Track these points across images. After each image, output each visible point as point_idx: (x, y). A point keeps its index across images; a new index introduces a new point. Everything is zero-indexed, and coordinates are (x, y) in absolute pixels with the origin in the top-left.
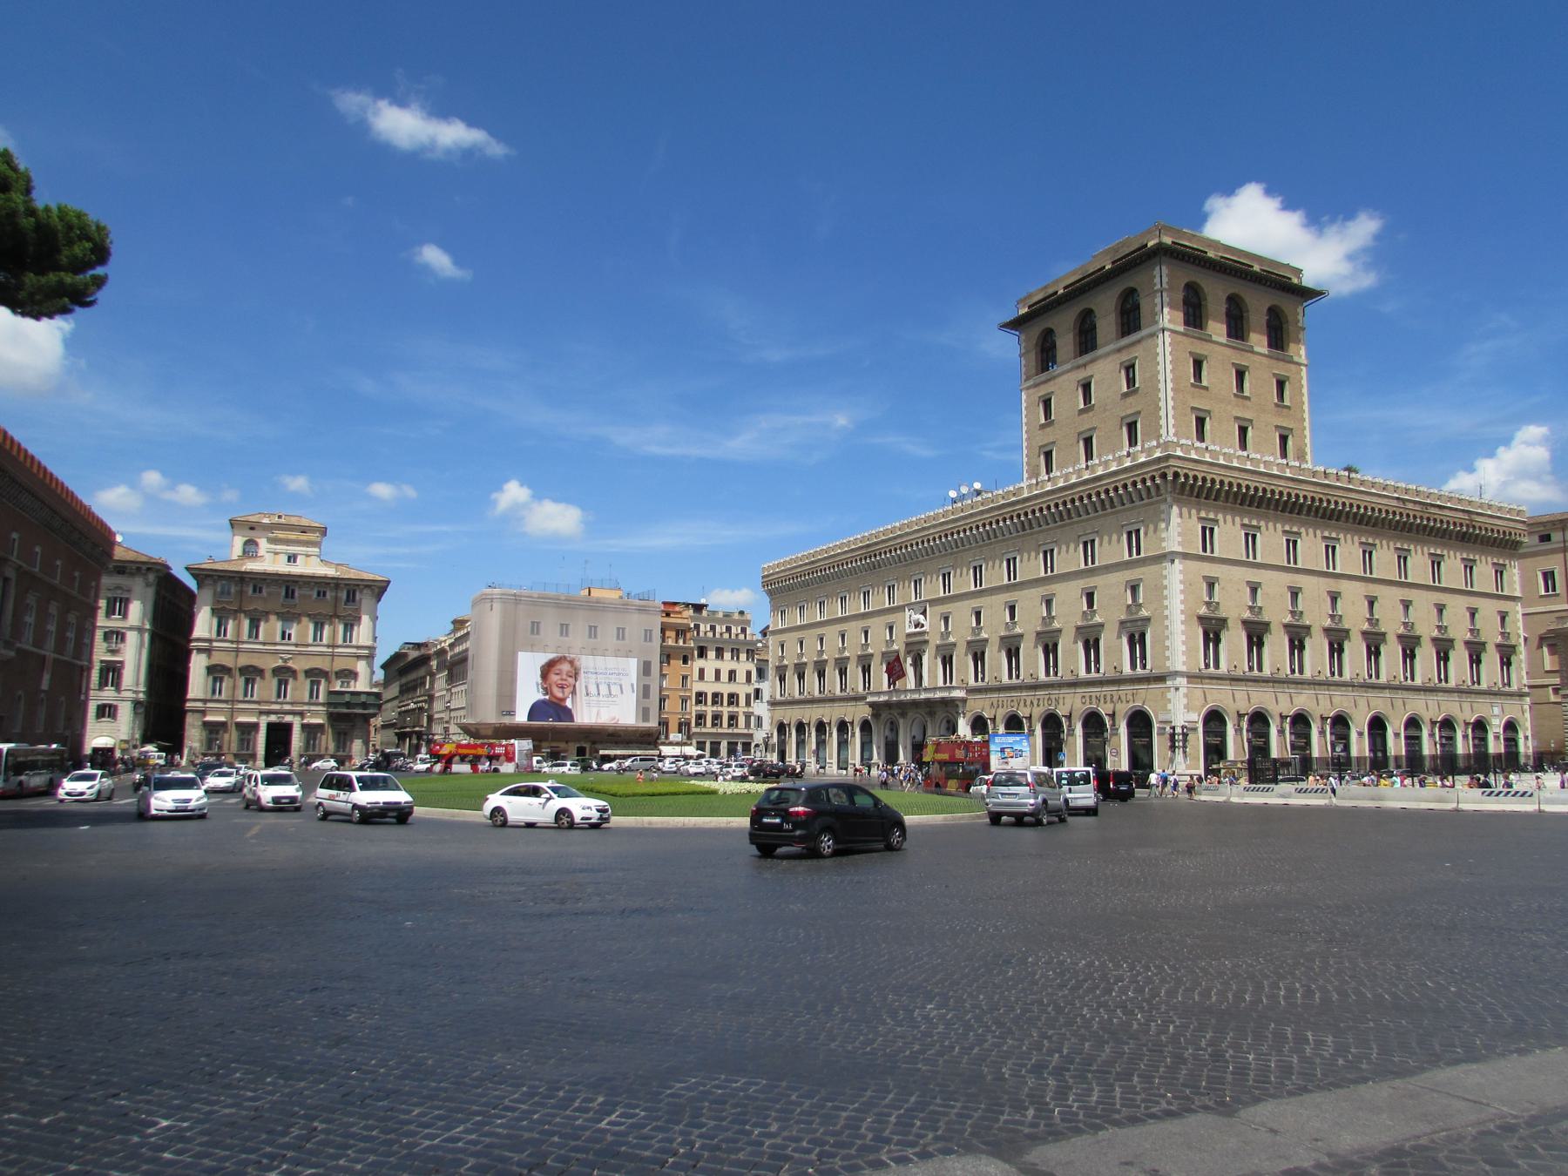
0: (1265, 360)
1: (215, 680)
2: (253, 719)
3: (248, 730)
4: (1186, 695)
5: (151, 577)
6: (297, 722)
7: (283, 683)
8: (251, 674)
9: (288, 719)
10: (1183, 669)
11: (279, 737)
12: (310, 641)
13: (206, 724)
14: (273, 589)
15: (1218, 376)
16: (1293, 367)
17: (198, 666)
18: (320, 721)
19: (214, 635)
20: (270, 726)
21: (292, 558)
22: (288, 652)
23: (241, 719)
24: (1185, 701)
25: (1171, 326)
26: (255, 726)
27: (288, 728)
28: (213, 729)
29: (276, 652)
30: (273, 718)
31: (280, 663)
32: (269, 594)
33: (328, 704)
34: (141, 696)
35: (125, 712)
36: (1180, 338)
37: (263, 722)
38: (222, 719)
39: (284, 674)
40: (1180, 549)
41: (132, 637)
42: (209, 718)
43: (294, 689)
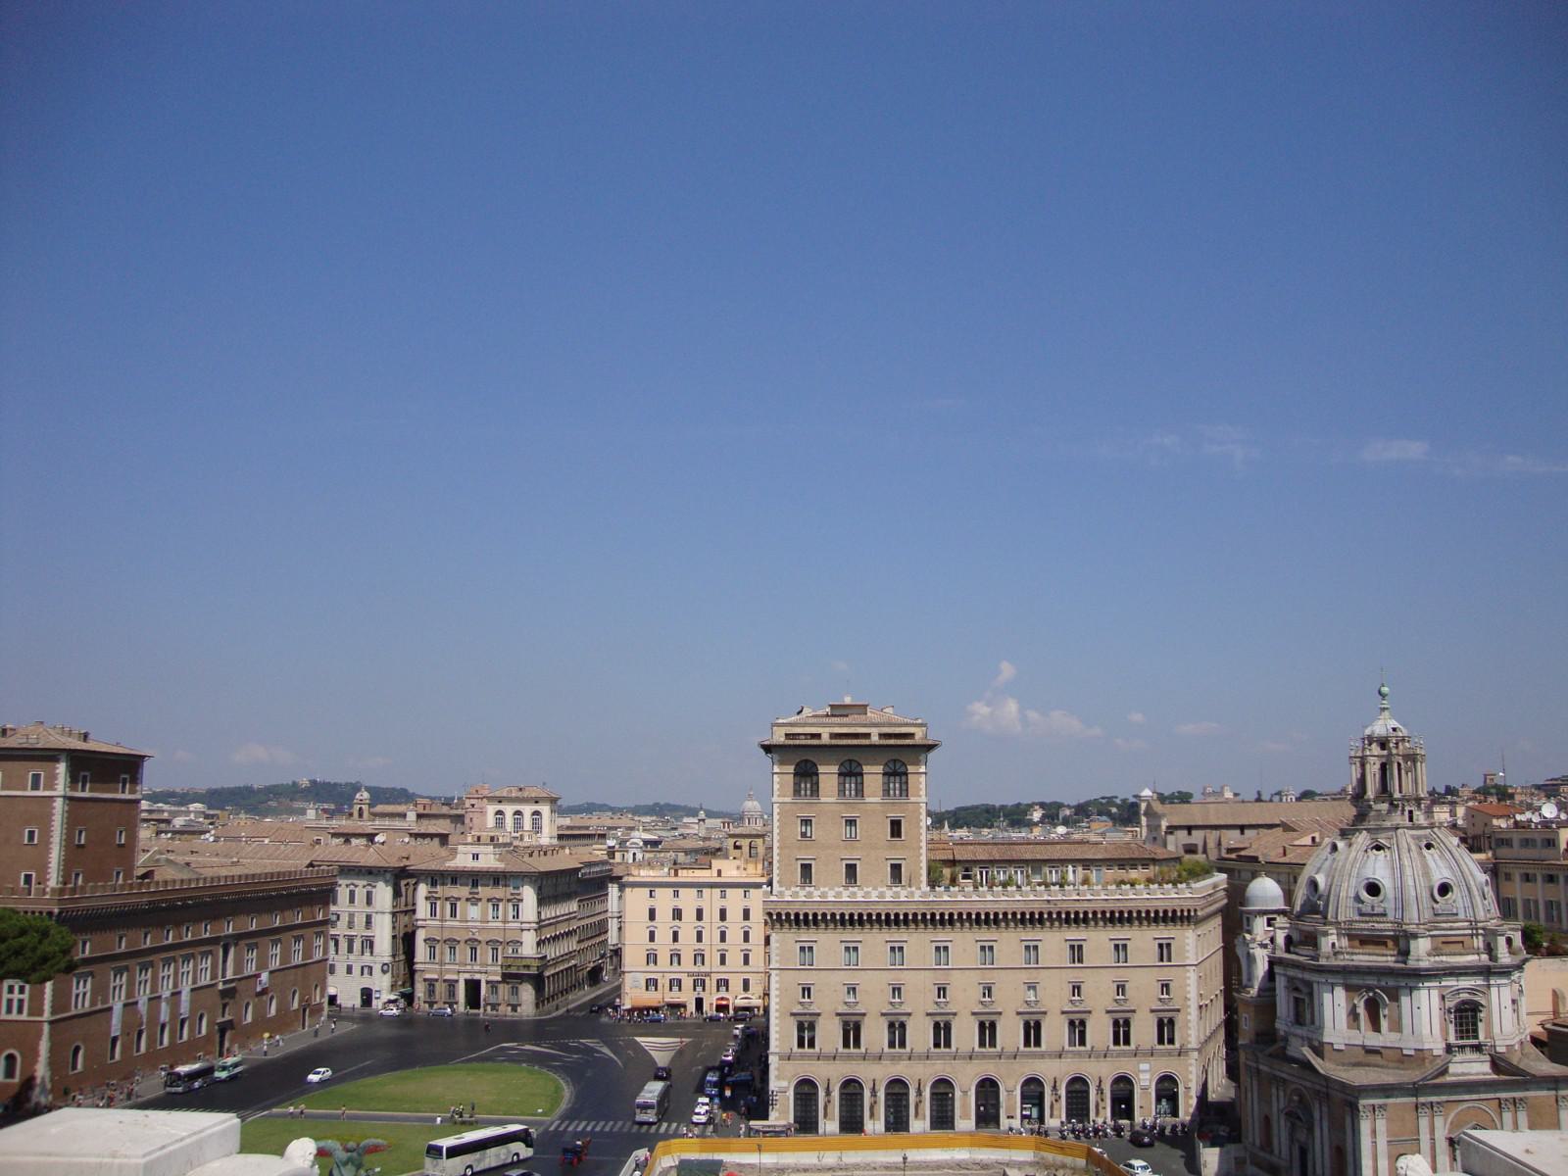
0: (879, 807)
1: (431, 947)
2: (455, 977)
3: (452, 985)
4: (778, 1069)
5: (388, 876)
6: (483, 978)
7: (474, 949)
8: (452, 944)
9: (477, 977)
10: (777, 1050)
11: (473, 987)
12: (490, 918)
13: (425, 980)
14: (464, 880)
15: (828, 830)
16: (910, 806)
17: (421, 935)
18: (499, 978)
19: (429, 917)
20: (467, 982)
21: (476, 857)
22: (475, 927)
23: (448, 977)
24: (777, 1073)
25: (781, 800)
26: (457, 981)
27: (478, 983)
28: (431, 983)
29: (467, 928)
30: (468, 976)
31: (470, 936)
34: (388, 960)
35: (377, 969)
36: (788, 807)
37: (462, 978)
38: (436, 977)
39: (473, 944)
40: (777, 966)
41: (376, 919)
42: (428, 976)
43: (481, 955)
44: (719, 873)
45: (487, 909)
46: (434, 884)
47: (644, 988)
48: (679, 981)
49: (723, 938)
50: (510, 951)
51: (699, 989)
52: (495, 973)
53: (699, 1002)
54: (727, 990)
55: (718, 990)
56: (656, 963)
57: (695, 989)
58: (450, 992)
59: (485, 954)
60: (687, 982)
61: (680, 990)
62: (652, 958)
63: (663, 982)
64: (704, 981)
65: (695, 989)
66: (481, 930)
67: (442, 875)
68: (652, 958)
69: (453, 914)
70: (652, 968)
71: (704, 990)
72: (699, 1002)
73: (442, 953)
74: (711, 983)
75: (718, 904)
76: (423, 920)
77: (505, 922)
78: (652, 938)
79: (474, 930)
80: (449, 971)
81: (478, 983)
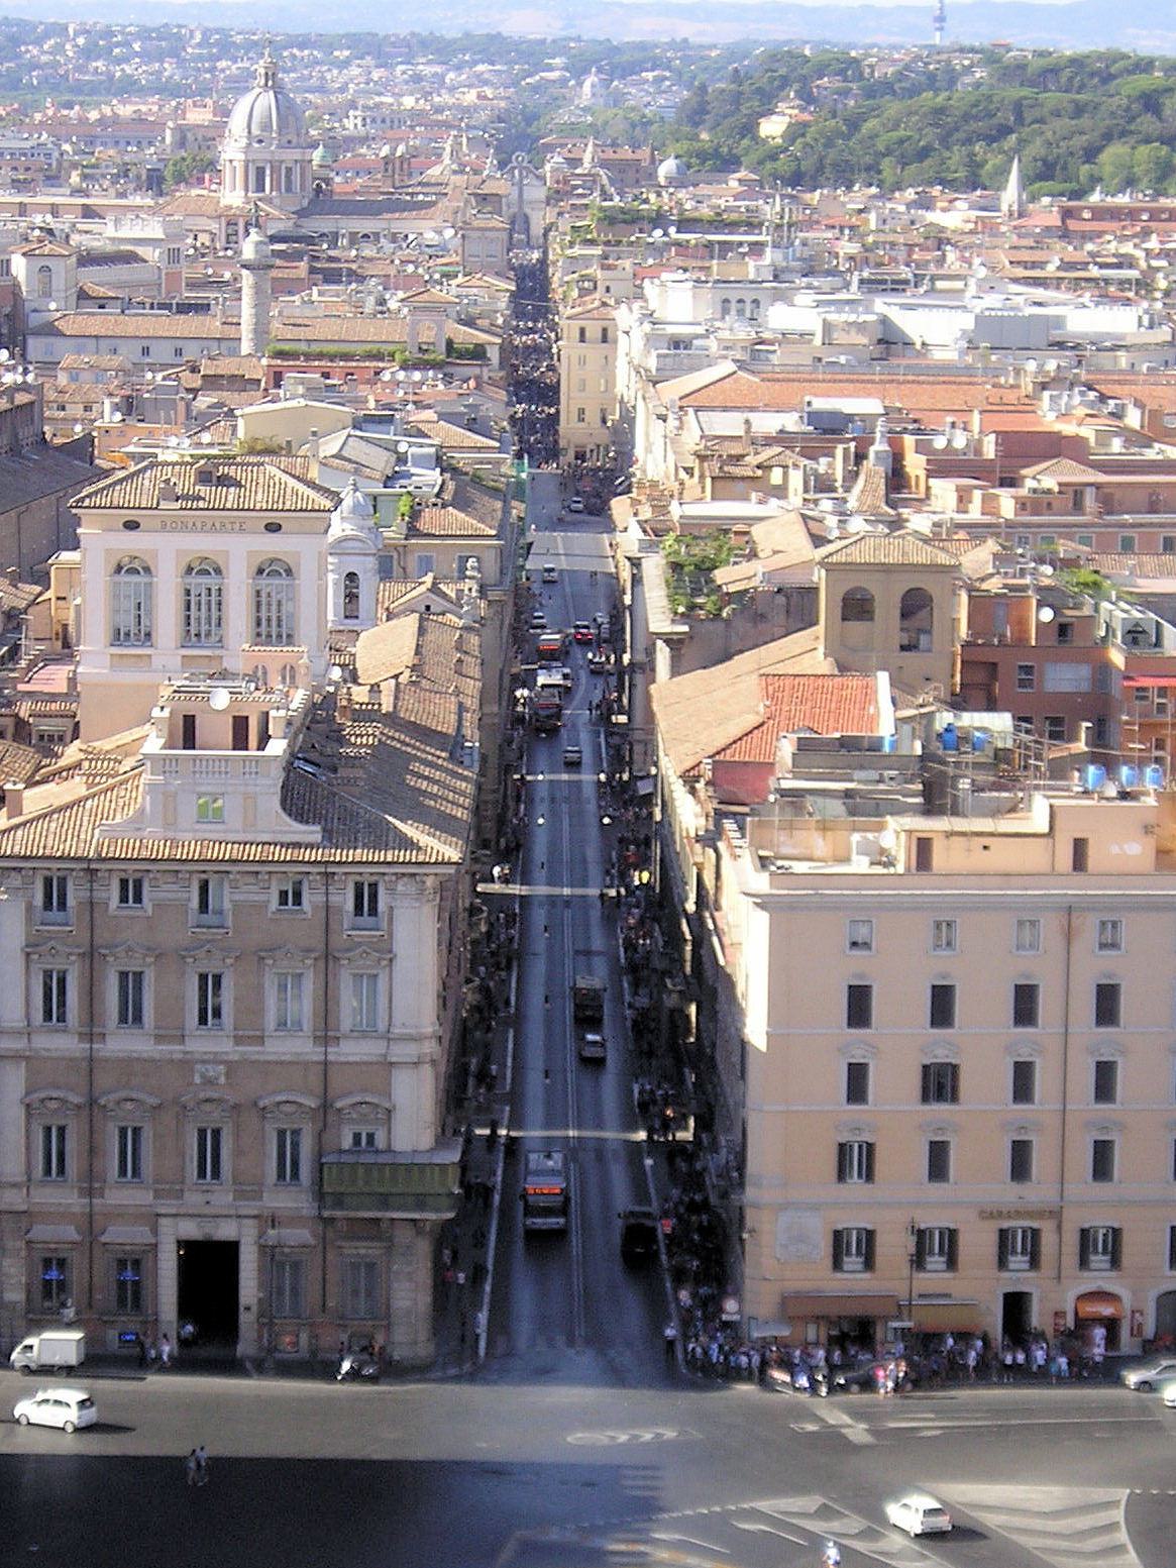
3: (133, 1267)
9: (225, 1231)
11: (209, 1269)
22: (216, 1060)
27: (230, 1249)
29: (186, 1064)
30: (191, 1230)
32: (157, 906)
33: (320, 1196)
38: (71, 1233)
42: (41, 1232)
43: (238, 1153)
44: (1080, 846)
45: (261, 986)
46: (54, 895)
47: (829, 1262)
48: (951, 1237)
49: (1104, 1088)
50: (347, 1142)
51: (1018, 1261)
52: (295, 1220)
53: (1015, 1305)
54: (1115, 1262)
55: (1084, 1263)
56: (869, 1175)
57: (1002, 1263)
58: (122, 1285)
59: (251, 1153)
60: (978, 1243)
61: (952, 1263)
62: (855, 1160)
63: (894, 1246)
64: (1036, 1233)
65: (1002, 1263)
66: (231, 1067)
67: (93, 872)
68: (855, 1160)
69: (132, 1013)
70: (855, 1185)
71: (1034, 1262)
72: (1015, 1305)
73: (92, 1151)
74: (1059, 1245)
75: (1091, 968)
76: (18, 1033)
77: (326, 1033)
78: (857, 1082)
79: (211, 1071)
80: (118, 1214)
81: (230, 1249)
